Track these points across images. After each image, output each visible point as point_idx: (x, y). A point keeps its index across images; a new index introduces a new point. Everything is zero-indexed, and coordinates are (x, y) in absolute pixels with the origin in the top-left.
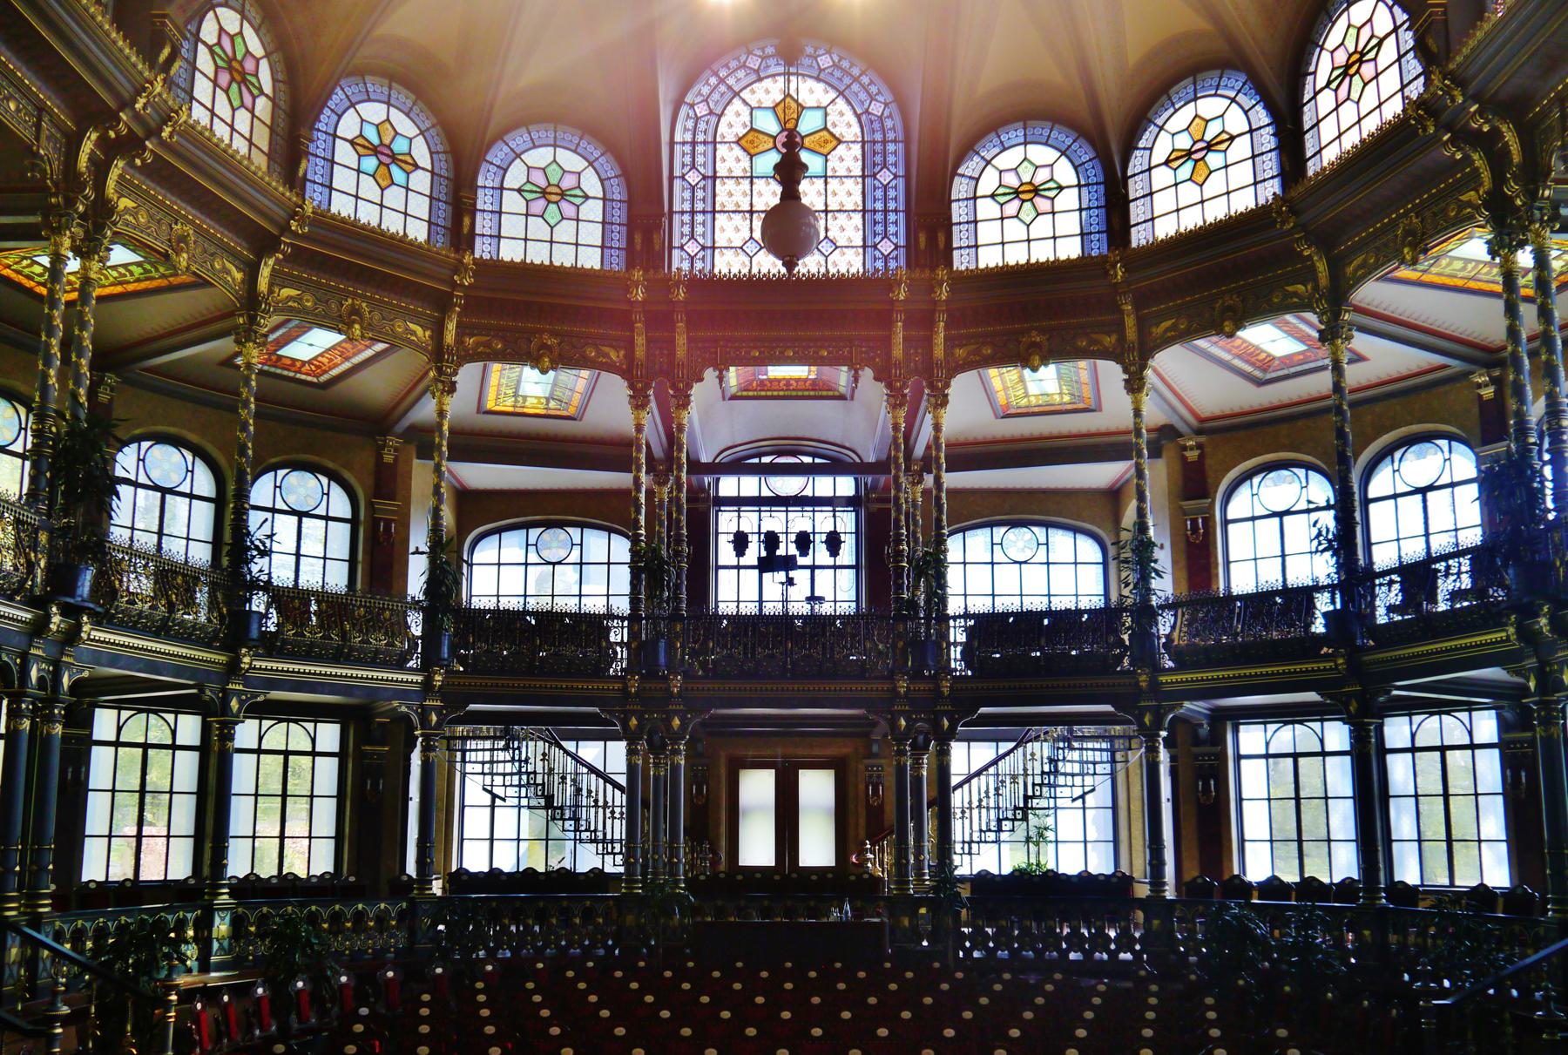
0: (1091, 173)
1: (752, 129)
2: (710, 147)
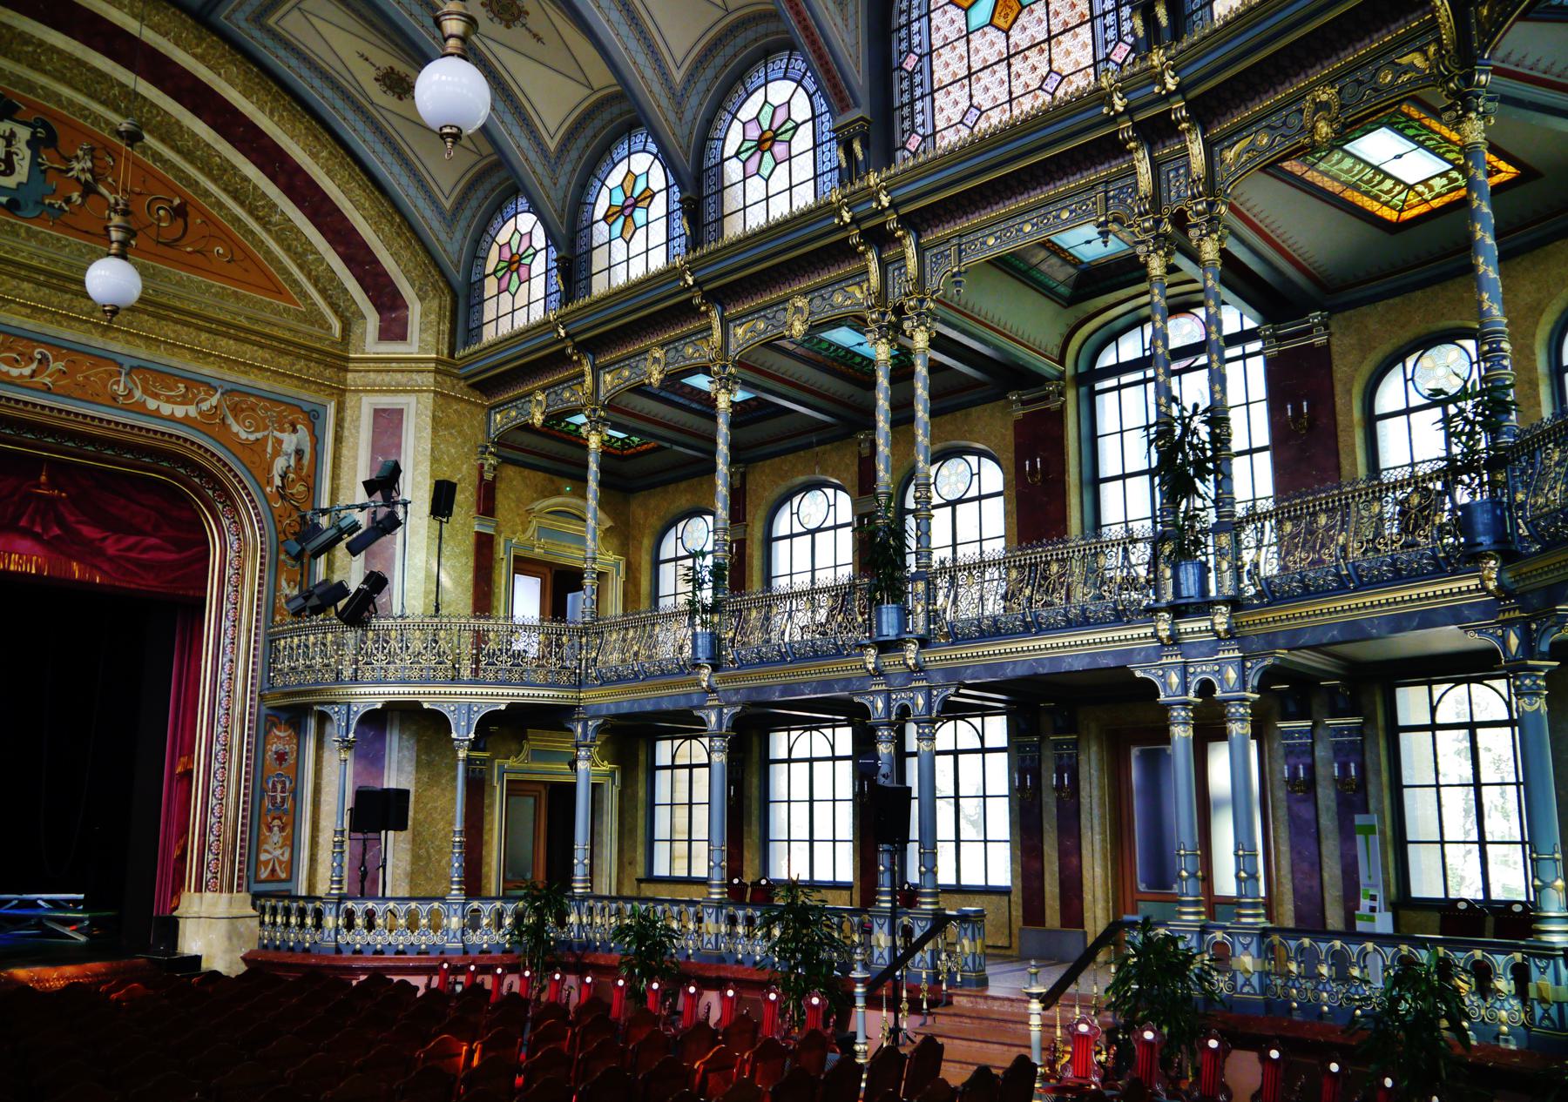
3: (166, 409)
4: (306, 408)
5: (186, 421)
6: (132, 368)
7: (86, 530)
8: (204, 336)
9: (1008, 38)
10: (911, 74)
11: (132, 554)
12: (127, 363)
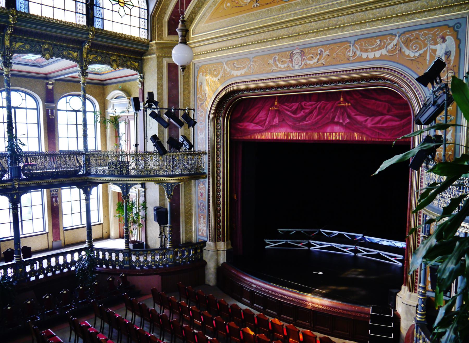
3: (371, 55)
4: (451, 24)
5: (382, 58)
6: (355, 41)
7: (359, 118)
8: (387, 9)
11: (379, 125)
12: (352, 40)
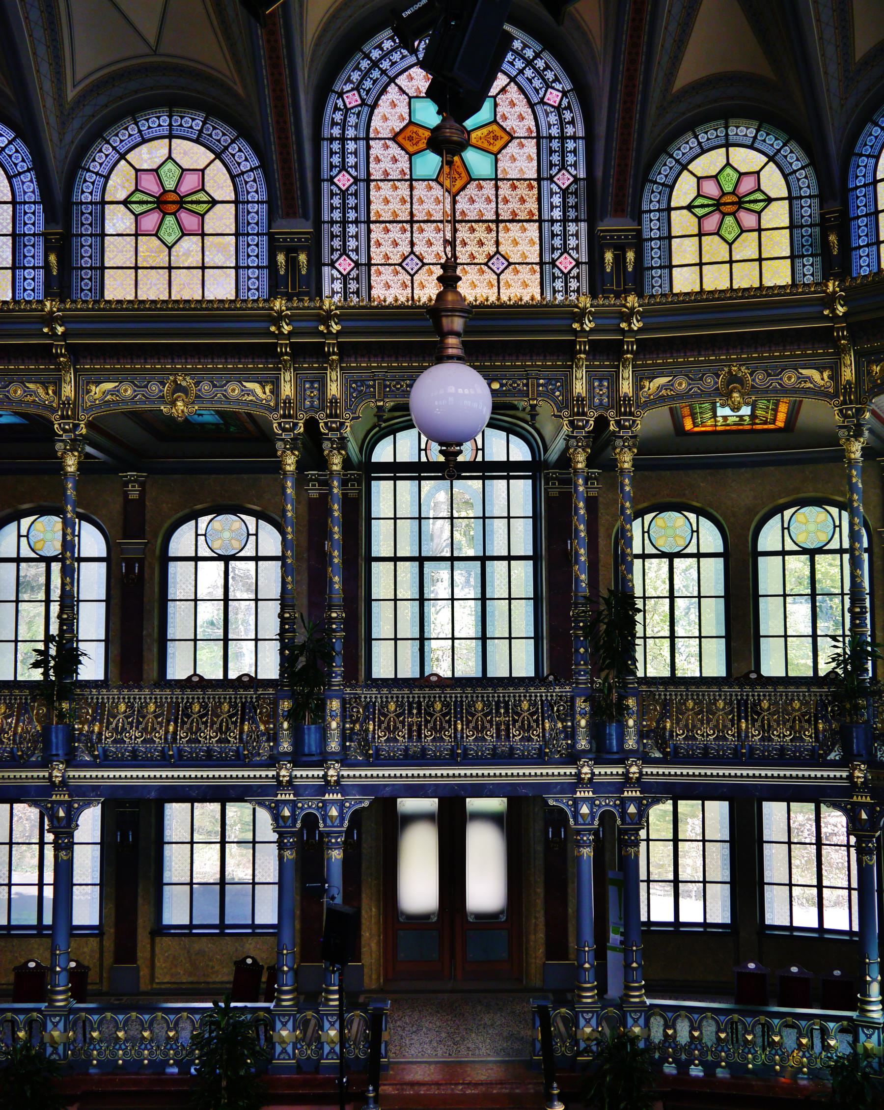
0: (804, 183)
1: (411, 123)
2: (362, 143)
9: (454, 202)
10: (344, 194)
